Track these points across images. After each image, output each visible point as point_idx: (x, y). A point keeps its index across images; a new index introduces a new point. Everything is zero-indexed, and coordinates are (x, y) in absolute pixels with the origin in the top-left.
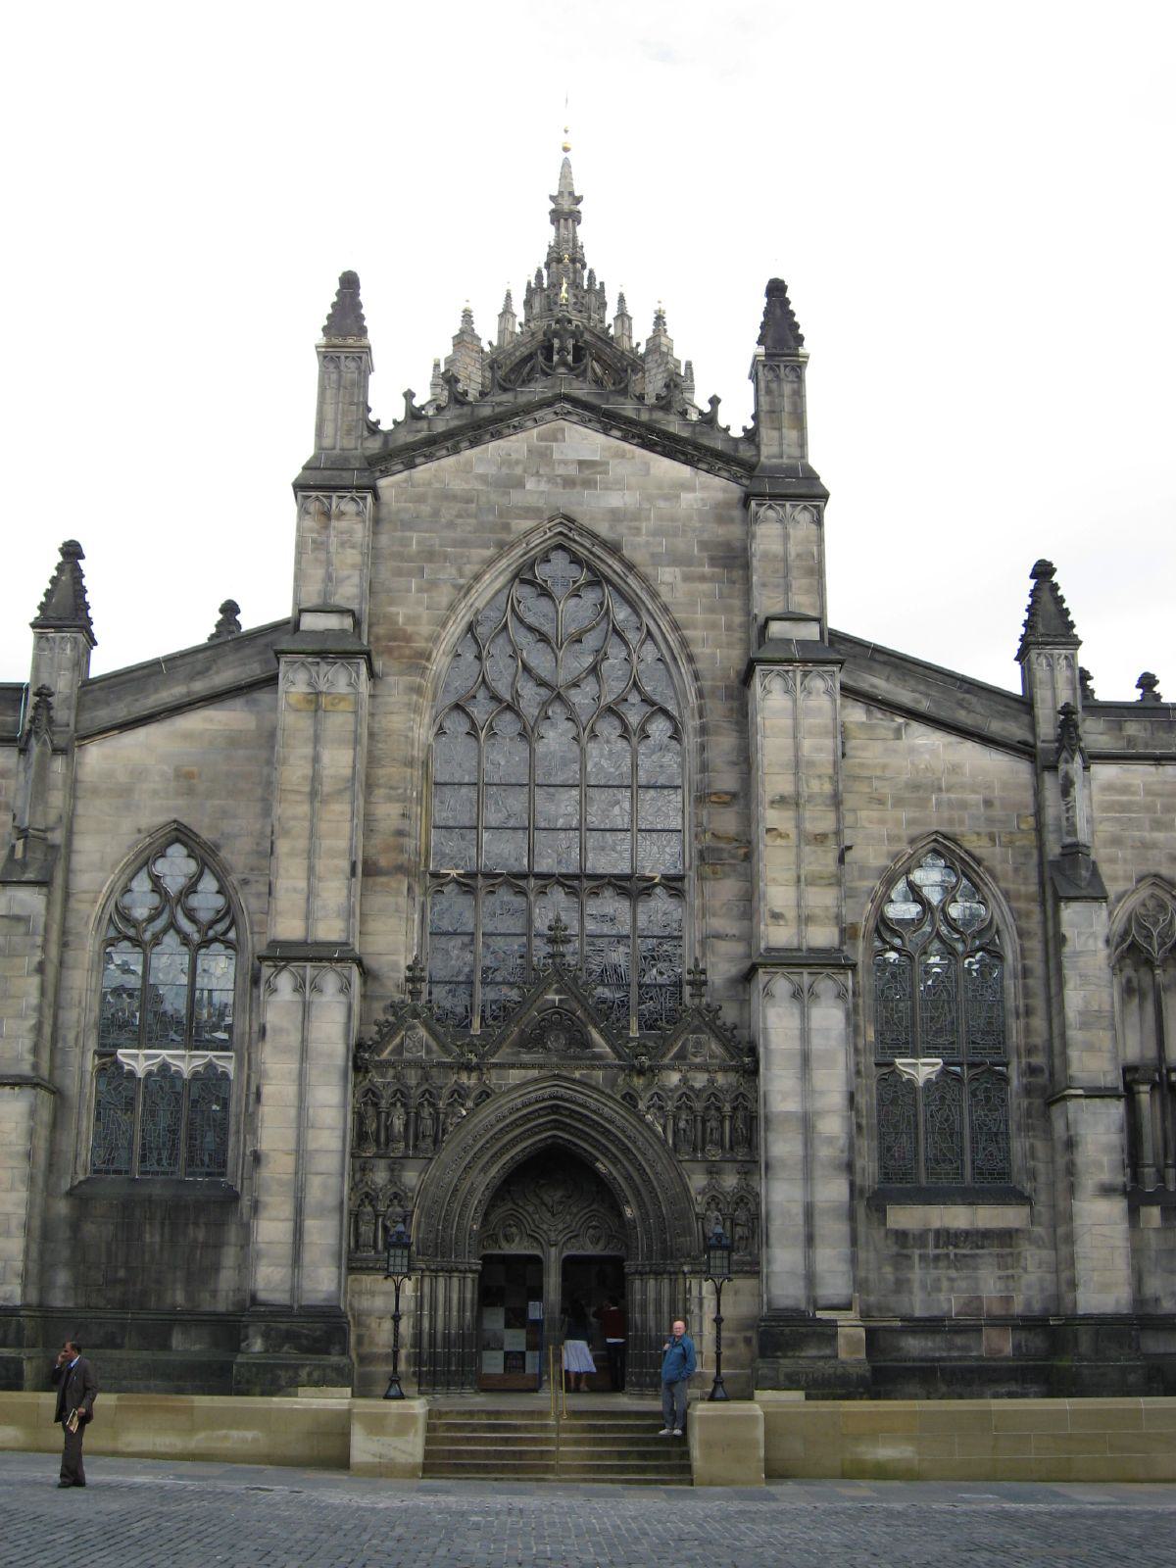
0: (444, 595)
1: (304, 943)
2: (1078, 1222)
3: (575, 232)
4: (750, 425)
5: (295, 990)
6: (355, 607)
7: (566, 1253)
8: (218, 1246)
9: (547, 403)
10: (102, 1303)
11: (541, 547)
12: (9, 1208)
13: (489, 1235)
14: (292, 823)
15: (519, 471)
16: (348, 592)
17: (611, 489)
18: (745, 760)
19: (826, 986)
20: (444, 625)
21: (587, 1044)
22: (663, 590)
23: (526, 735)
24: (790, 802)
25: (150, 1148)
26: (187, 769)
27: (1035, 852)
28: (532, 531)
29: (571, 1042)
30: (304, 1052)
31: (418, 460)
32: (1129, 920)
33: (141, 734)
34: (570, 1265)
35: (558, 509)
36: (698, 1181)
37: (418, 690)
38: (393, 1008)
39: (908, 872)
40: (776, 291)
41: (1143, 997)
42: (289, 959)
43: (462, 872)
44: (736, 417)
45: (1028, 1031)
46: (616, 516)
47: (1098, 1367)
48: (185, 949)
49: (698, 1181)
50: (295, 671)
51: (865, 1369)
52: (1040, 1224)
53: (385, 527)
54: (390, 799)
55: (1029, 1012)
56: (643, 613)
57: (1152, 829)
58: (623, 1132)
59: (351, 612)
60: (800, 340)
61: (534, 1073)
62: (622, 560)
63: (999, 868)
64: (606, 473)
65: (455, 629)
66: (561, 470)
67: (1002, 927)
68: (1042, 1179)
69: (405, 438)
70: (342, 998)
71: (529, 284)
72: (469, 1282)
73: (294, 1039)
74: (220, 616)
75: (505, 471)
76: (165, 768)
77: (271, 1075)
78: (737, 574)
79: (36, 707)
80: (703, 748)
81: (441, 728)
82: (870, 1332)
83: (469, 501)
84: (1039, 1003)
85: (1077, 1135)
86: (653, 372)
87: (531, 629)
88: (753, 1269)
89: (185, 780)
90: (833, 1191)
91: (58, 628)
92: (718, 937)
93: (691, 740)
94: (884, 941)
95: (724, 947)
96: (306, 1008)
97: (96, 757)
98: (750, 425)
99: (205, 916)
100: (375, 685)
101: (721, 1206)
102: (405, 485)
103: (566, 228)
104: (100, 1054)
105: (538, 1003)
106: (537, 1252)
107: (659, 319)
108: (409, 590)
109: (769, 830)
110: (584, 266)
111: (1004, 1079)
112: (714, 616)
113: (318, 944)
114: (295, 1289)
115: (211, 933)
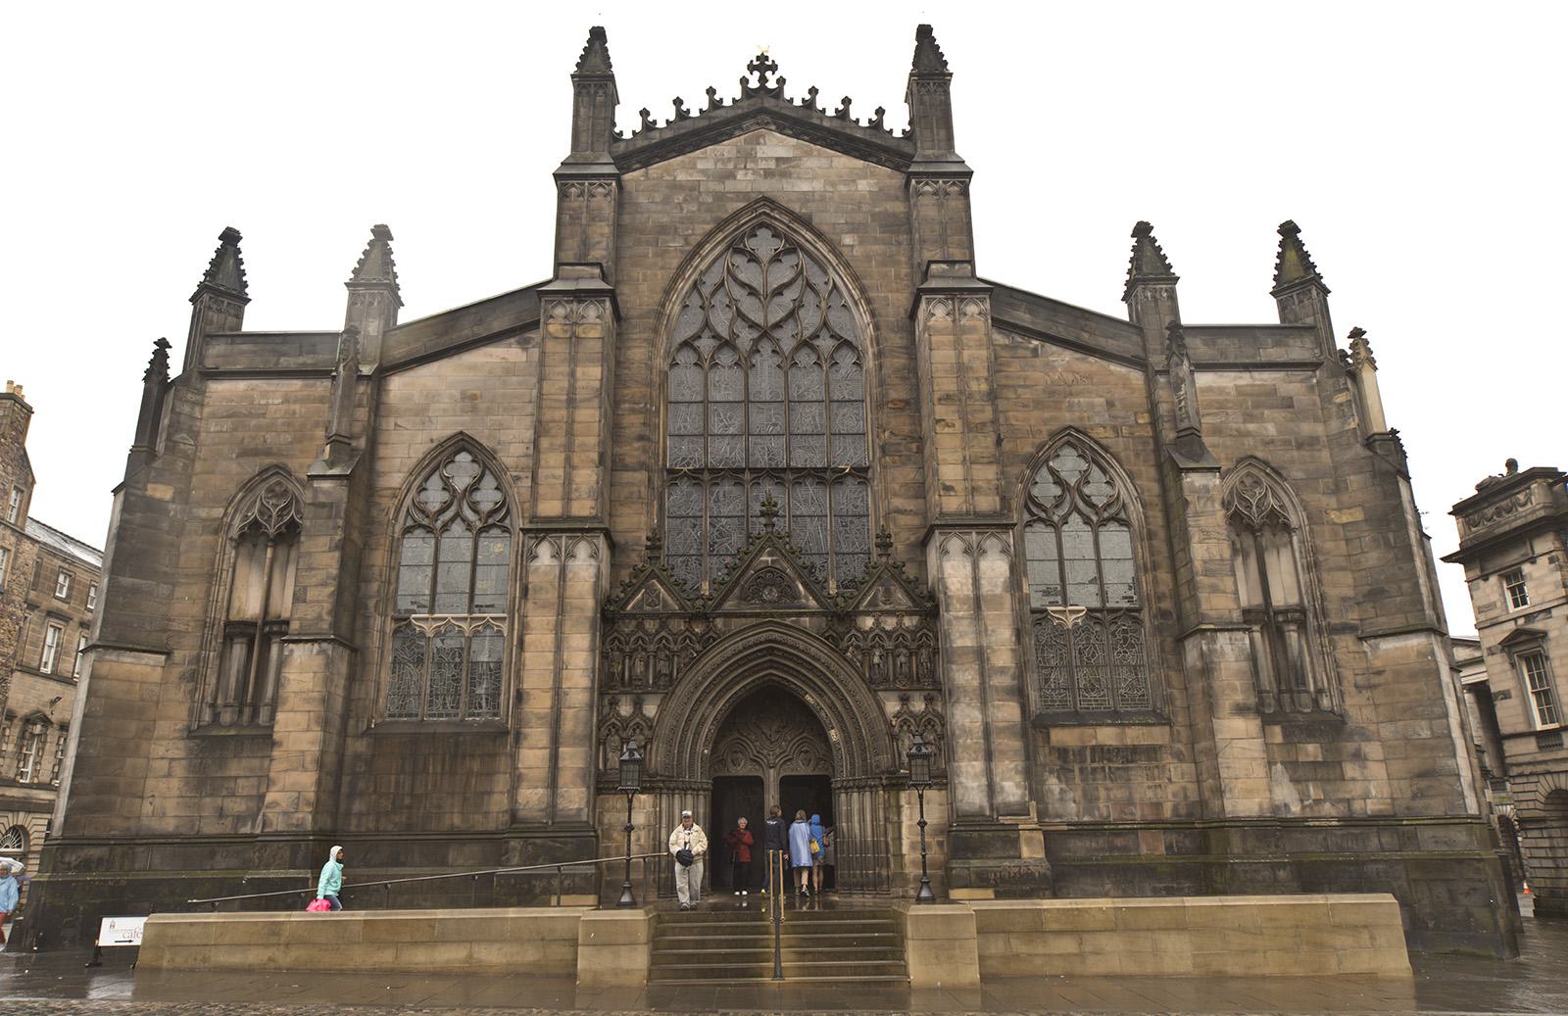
2: (1219, 737)
4: (908, 128)
5: (553, 556)
7: (783, 774)
8: (489, 774)
10: (390, 827)
12: (305, 747)
13: (716, 758)
14: (551, 425)
15: (731, 166)
17: (799, 178)
18: (913, 372)
19: (992, 544)
21: (796, 596)
22: (845, 251)
23: (745, 364)
24: (957, 398)
25: (437, 695)
26: (470, 392)
27: (1151, 441)
28: (743, 209)
29: (782, 594)
32: (1231, 492)
33: (434, 368)
34: (786, 783)
35: (761, 192)
36: (892, 706)
38: (637, 572)
39: (1047, 461)
40: (924, 33)
41: (1246, 557)
44: (898, 121)
45: (1155, 581)
46: (806, 198)
47: (1250, 864)
48: (469, 534)
49: (892, 706)
51: (1044, 868)
52: (1179, 742)
54: (633, 411)
55: (1155, 567)
56: (830, 270)
57: (1245, 421)
58: (828, 668)
60: (946, 63)
61: (754, 621)
63: (1122, 455)
65: (684, 286)
66: (763, 165)
67: (1128, 500)
68: (1178, 703)
70: (593, 562)
72: (702, 797)
73: (552, 596)
75: (719, 165)
76: (454, 392)
77: (533, 626)
78: (903, 238)
80: (881, 367)
81: (674, 359)
82: (1045, 833)
83: (692, 189)
84: (1162, 556)
85: (1212, 662)
87: (743, 285)
88: (943, 780)
89: (470, 400)
90: (1008, 712)
92: (898, 511)
93: (870, 363)
94: (1032, 513)
95: (903, 520)
97: (397, 385)
98: (908, 128)
99: (486, 507)
100: (619, 326)
101: (912, 728)
105: (755, 564)
106: (760, 774)
108: (646, 256)
109: (938, 421)
111: (1138, 621)
112: (885, 269)
114: (553, 805)
115: (490, 521)
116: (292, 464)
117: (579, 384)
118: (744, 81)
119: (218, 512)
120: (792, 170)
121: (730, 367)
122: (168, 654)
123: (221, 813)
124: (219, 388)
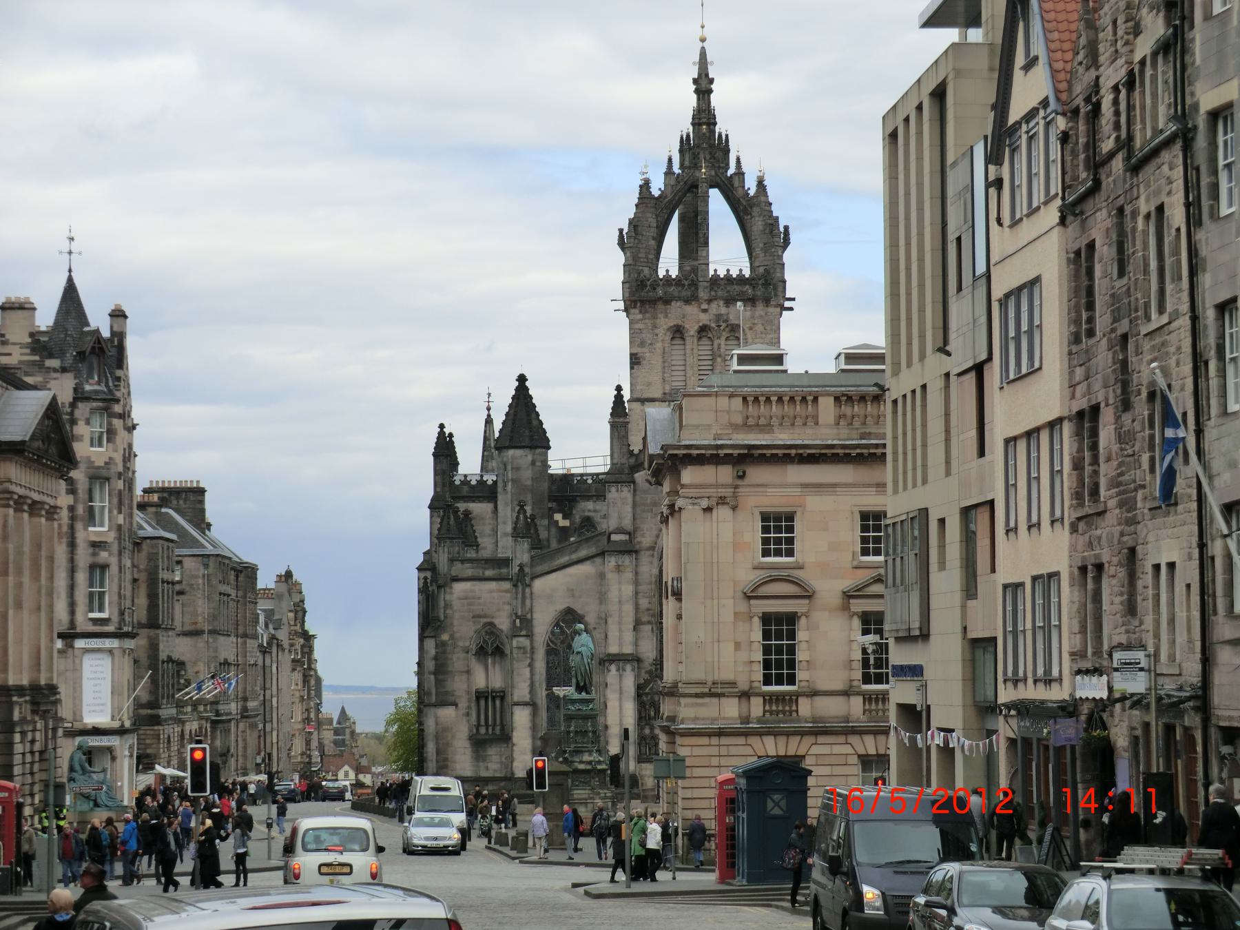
1: (618, 655)
3: (709, 102)
16: (627, 523)
30: (621, 693)
33: (554, 575)
38: (650, 672)
42: (614, 661)
53: (638, 493)
59: (629, 534)
71: (682, 138)
74: (517, 383)
89: (571, 592)
91: (522, 538)
96: (621, 676)
97: (538, 584)
103: (703, 98)
104: (546, 690)
107: (761, 184)
110: (715, 124)
113: (623, 655)
116: (496, 622)
119: (467, 644)
122: (456, 705)
123: (487, 768)
124: (459, 587)
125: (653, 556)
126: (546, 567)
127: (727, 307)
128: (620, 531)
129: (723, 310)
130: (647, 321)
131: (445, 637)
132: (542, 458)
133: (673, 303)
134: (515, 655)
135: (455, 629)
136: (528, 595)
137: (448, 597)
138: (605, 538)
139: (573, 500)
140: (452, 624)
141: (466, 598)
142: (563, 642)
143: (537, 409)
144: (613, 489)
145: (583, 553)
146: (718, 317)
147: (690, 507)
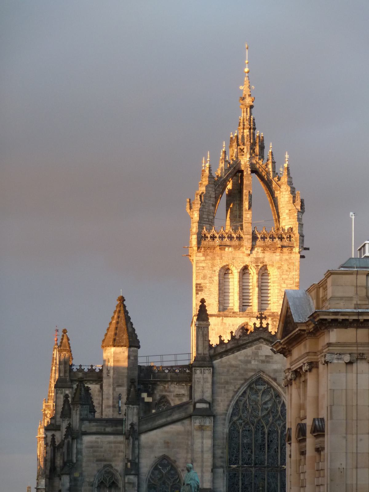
0: (231, 394)
6: (209, 399)
9: (258, 340)
11: (256, 378)
15: (250, 358)
16: (208, 396)
17: (274, 363)
20: (231, 402)
28: (254, 375)
31: (223, 356)
33: (154, 432)
37: (225, 420)
43: (236, 466)
46: (276, 371)
50: (196, 420)
59: (209, 403)
62: (277, 383)
64: (272, 359)
65: (233, 403)
66: (261, 358)
69: (220, 350)
75: (246, 358)
79: (130, 428)
81: (230, 428)
83: (236, 367)
86: (284, 193)
89: (167, 444)
91: (133, 405)
97: (144, 438)
102: (220, 363)
108: (222, 392)
116: (113, 464)
117: (205, 445)
118: (255, 324)
119: (92, 480)
120: (271, 360)
121: (249, 430)
124: (87, 439)
125: (225, 420)
126: (149, 426)
127: (263, 253)
128: (202, 401)
129: (261, 255)
130: (208, 261)
131: (76, 475)
132: (134, 354)
133: (227, 249)
134: (126, 488)
135: (83, 469)
136: (137, 446)
137: (79, 446)
138: (191, 407)
139: (155, 384)
140: (81, 465)
141: (92, 447)
142: (160, 479)
143: (131, 321)
144: (198, 372)
145: (176, 416)
146: (257, 259)
147: (335, 361)
